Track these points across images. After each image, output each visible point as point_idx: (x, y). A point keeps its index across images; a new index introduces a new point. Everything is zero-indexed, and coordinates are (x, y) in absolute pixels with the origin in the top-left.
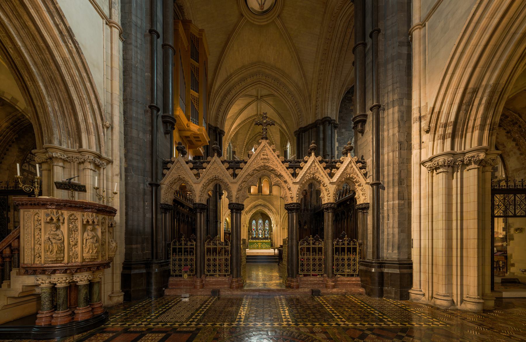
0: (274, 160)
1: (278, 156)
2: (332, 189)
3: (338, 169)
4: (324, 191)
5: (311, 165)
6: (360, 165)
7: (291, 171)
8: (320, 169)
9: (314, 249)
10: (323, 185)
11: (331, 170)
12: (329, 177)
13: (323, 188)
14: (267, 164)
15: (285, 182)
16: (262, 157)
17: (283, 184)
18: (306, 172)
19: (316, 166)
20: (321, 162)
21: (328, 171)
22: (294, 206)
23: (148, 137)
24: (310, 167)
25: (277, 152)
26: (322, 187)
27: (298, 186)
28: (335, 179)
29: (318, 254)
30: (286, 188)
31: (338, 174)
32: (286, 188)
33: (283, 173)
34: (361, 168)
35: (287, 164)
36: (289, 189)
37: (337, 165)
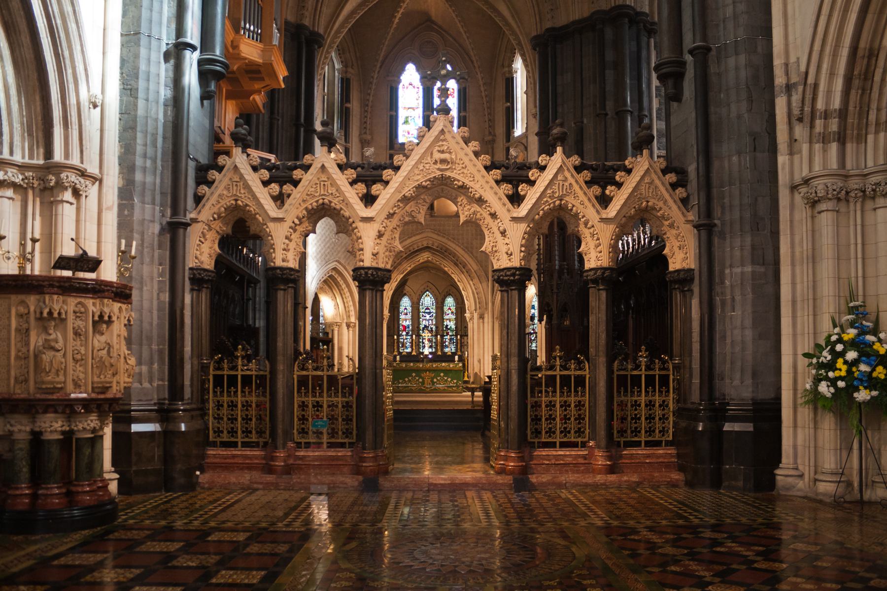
0: (467, 162)
1: (477, 154)
3: (619, 185)
4: (589, 239)
5: (556, 176)
8: (576, 187)
9: (566, 380)
10: (586, 224)
12: (597, 206)
13: (585, 233)
14: (448, 174)
16: (437, 156)
17: (489, 219)
19: (566, 179)
20: (578, 169)
21: (596, 190)
22: (514, 275)
24: (551, 181)
25: (474, 145)
26: (582, 227)
29: (576, 391)
30: (495, 229)
31: (619, 198)
32: (495, 229)
36: (503, 233)
37: (617, 178)
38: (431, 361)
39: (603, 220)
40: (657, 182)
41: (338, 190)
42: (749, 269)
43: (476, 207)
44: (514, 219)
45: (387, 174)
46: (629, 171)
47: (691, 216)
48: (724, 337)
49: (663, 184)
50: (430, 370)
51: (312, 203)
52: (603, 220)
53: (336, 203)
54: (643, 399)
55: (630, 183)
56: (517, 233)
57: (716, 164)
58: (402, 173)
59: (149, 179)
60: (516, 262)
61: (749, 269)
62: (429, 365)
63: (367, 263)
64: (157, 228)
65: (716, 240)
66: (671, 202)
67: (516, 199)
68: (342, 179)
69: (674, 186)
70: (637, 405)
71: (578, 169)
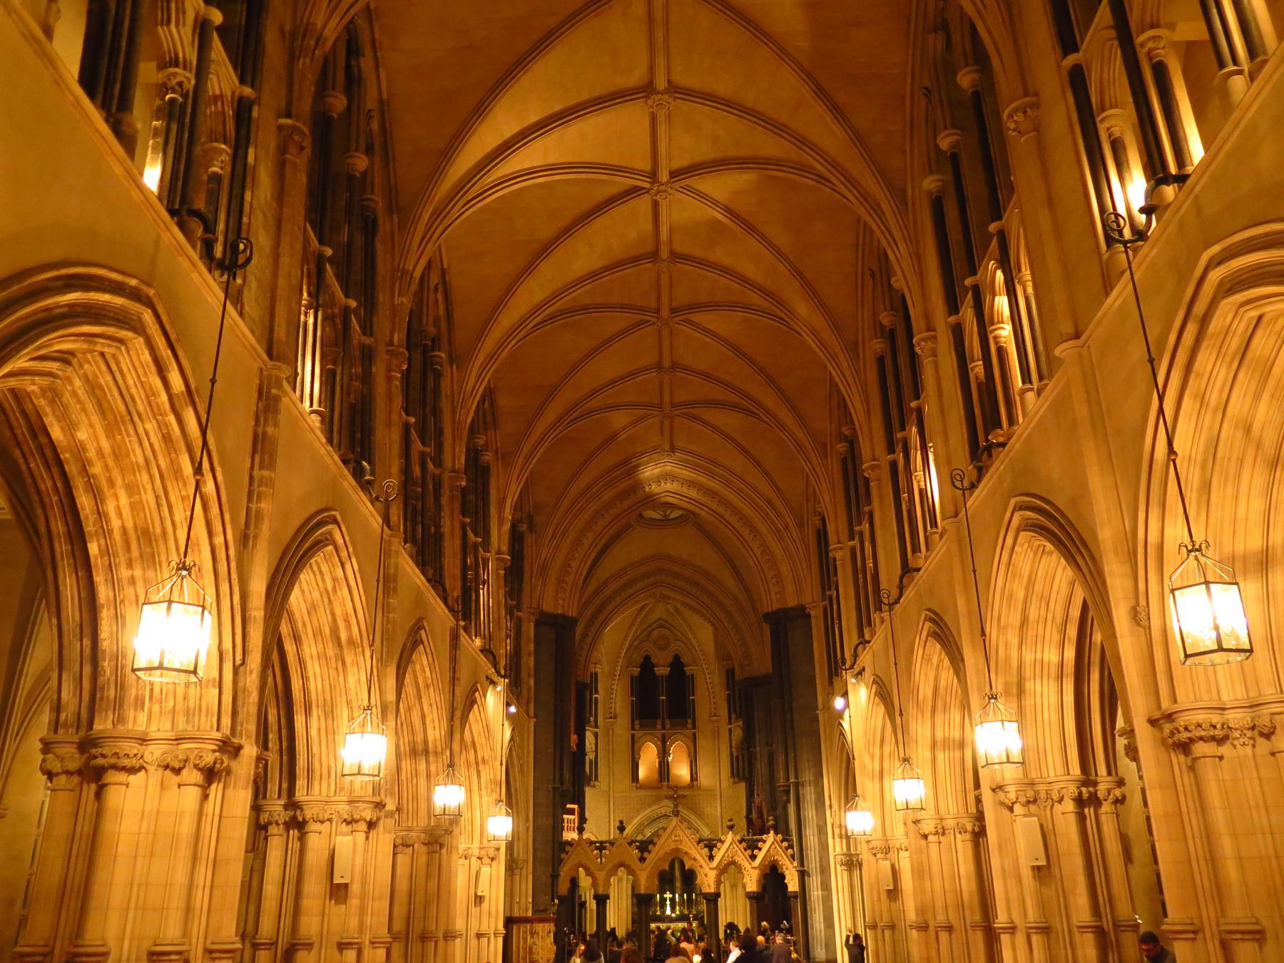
3: (760, 849)
6: (785, 844)
8: (739, 851)
11: (753, 851)
15: (701, 867)
16: (674, 838)
21: (749, 852)
23: (550, 821)
27: (715, 872)
28: (757, 862)
33: (698, 857)
34: (787, 848)
36: (706, 875)
39: (753, 868)
40: (778, 848)
43: (693, 862)
44: (711, 869)
45: (651, 847)
46: (764, 842)
47: (795, 864)
49: (781, 848)
51: (616, 862)
52: (753, 868)
53: (628, 863)
55: (765, 848)
56: (712, 875)
58: (657, 848)
60: (712, 890)
63: (643, 892)
66: (785, 857)
67: (711, 858)
69: (787, 848)
71: (740, 842)
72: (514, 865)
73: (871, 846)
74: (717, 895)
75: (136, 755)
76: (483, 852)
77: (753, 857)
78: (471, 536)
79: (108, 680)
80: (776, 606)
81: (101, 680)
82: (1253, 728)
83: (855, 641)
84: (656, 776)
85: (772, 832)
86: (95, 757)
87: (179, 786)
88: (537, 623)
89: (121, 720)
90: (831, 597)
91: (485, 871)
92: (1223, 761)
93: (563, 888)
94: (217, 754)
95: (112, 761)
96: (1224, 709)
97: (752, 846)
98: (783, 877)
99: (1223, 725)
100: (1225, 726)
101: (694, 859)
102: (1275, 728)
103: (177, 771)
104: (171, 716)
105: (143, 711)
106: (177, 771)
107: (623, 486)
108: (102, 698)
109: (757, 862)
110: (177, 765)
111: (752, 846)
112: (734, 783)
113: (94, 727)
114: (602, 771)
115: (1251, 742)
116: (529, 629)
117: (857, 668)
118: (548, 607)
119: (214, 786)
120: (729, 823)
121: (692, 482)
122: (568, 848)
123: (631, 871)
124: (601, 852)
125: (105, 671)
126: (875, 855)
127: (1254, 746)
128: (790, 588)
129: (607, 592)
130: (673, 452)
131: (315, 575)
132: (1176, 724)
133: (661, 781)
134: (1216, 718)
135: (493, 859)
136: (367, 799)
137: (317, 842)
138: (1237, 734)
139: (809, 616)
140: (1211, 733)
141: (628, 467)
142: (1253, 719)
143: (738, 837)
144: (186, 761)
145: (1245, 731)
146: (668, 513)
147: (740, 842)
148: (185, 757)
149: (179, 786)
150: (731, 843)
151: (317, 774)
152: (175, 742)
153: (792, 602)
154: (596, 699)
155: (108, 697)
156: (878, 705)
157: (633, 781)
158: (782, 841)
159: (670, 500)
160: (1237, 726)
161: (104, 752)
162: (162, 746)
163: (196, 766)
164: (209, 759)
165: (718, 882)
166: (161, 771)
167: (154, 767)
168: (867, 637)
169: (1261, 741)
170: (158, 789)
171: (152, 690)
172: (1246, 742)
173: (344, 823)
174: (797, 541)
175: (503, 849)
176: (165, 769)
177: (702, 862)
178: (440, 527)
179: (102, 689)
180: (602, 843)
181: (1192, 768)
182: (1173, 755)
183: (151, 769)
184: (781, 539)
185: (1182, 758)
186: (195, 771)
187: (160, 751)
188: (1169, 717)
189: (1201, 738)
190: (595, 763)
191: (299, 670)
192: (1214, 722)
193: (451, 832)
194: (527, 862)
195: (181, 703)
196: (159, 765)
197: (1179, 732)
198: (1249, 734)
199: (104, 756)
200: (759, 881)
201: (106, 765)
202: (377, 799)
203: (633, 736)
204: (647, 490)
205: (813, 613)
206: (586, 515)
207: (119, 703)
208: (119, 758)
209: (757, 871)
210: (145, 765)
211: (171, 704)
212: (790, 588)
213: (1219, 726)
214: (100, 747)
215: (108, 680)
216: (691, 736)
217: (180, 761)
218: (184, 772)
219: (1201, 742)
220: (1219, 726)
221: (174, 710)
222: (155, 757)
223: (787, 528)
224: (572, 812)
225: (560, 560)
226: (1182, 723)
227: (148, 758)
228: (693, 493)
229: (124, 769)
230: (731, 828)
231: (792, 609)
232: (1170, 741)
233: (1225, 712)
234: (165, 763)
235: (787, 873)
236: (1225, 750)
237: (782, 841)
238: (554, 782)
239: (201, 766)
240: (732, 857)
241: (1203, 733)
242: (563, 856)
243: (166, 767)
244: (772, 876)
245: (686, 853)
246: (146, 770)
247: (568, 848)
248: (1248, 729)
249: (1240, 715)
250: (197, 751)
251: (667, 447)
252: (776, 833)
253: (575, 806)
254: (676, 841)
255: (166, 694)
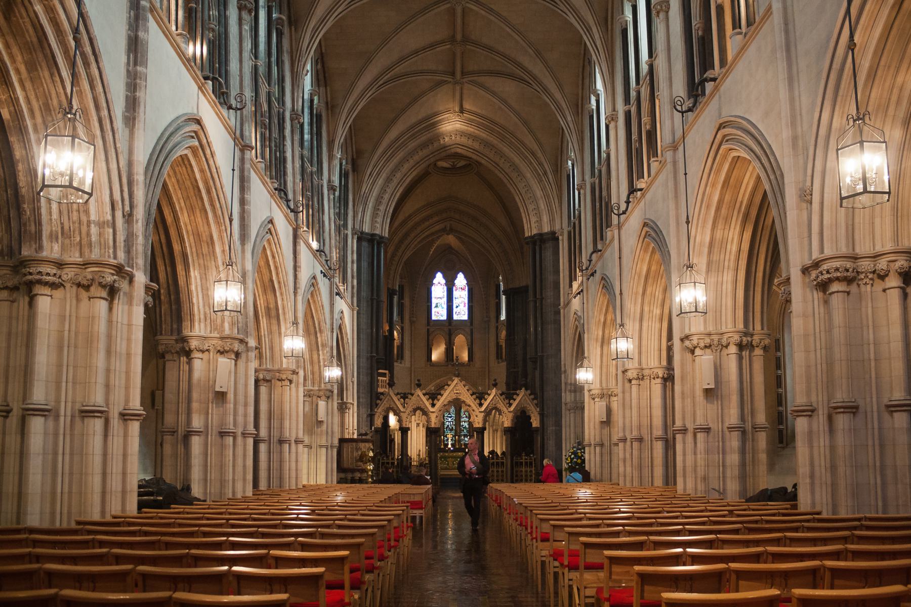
1: (468, 390)
2: (510, 416)
3: (515, 400)
6: (532, 397)
7: (478, 401)
8: (500, 401)
11: (510, 401)
15: (473, 410)
16: (455, 391)
18: (489, 404)
21: (507, 401)
23: (369, 379)
28: (512, 408)
33: (472, 405)
34: (533, 399)
35: (474, 396)
36: (477, 416)
38: (452, 451)
39: (509, 412)
41: (423, 402)
42: (554, 428)
46: (518, 395)
47: (538, 410)
48: (547, 450)
50: (452, 457)
51: (415, 407)
52: (509, 412)
53: (422, 407)
54: (524, 469)
57: (545, 393)
58: (444, 397)
59: (364, 400)
60: (480, 425)
61: (554, 428)
62: (451, 454)
64: (365, 416)
65: (545, 419)
67: (481, 405)
68: (424, 399)
69: (533, 399)
70: (521, 471)
71: (501, 395)
72: (344, 406)
73: (591, 393)
74: (484, 429)
75: (55, 275)
76: (321, 393)
77: (510, 405)
78: (307, 165)
79: (29, 218)
80: (535, 232)
81: (25, 218)
82: (874, 272)
83: (590, 248)
84: (443, 357)
85: (523, 389)
86: (25, 275)
87: (90, 298)
88: (360, 240)
89: (40, 248)
90: (574, 224)
91: (322, 404)
92: (851, 295)
93: (378, 422)
94: (115, 277)
95: (38, 277)
96: (856, 259)
97: (509, 396)
98: (530, 418)
99: (854, 270)
100: (855, 270)
101: (469, 406)
102: (889, 271)
103: (87, 288)
104: (78, 248)
105: (58, 243)
106: (87, 288)
107: (423, 138)
108: (25, 231)
109: (512, 408)
110: (85, 282)
111: (509, 396)
112: (498, 363)
113: (22, 253)
114: (407, 354)
115: (871, 282)
116: (352, 243)
117: (590, 272)
118: (367, 229)
119: (116, 301)
120: (494, 383)
121: (475, 137)
122: (382, 397)
123: (425, 413)
124: (404, 400)
125: (25, 211)
126: (594, 399)
127: (872, 285)
128: (545, 219)
129: (410, 224)
130: (463, 113)
131: (186, 168)
132: (820, 269)
133: (447, 361)
134: (849, 265)
135: (328, 398)
136: (233, 336)
137: (198, 365)
138: (862, 276)
139: (558, 239)
140: (845, 275)
141: (429, 123)
142: (875, 265)
143: (500, 392)
144: (93, 280)
145: (868, 274)
146: (456, 163)
147: (501, 395)
148: (91, 277)
149: (90, 298)
150: (495, 396)
151: (197, 318)
152: (83, 267)
153: (546, 229)
154: (402, 303)
155: (30, 232)
156: (604, 295)
157: (428, 361)
158: (530, 395)
159: (459, 151)
160: (863, 270)
161: (31, 271)
162: (73, 269)
163: (100, 284)
164: (109, 279)
165: (485, 420)
166: (75, 288)
167: (69, 285)
168: (599, 247)
169: (877, 281)
170: (74, 302)
171: (62, 228)
172: (868, 282)
173: (218, 354)
174: (553, 185)
175: (336, 391)
176: (78, 287)
177: (475, 408)
178: (284, 152)
179: (25, 224)
180: (405, 394)
181: (826, 302)
182: (815, 293)
183: (68, 285)
184: (540, 181)
185: (821, 294)
186: (100, 288)
187: (73, 273)
188: (816, 265)
189: (837, 279)
190: (401, 347)
191: (179, 242)
192: (848, 266)
193: (297, 373)
194: (353, 404)
195: (86, 239)
196: (73, 283)
197: (822, 274)
198: (871, 276)
199: (31, 274)
200: (512, 420)
201: (34, 280)
202: (241, 336)
203: (428, 330)
204: (442, 142)
205: (560, 238)
206: (395, 160)
207: (38, 236)
208: (42, 275)
209: (512, 414)
210: (63, 283)
211: (78, 239)
212: (545, 219)
213: (851, 270)
214: (29, 268)
215: (29, 218)
216: (469, 333)
217: (88, 280)
218: (92, 289)
219: (837, 282)
220: (851, 270)
221: (80, 243)
222: (69, 276)
223: (545, 173)
224: (384, 375)
225: (375, 193)
226: (825, 268)
227: (65, 277)
228: (476, 145)
229: (46, 284)
230: (495, 385)
231: (546, 233)
232: (815, 283)
233: (857, 261)
234: (77, 282)
235: (532, 415)
236: (853, 288)
237: (530, 395)
238: (371, 353)
239: (104, 283)
240: (495, 405)
241: (839, 274)
242: (378, 401)
243: (79, 285)
244: (522, 418)
245: (464, 402)
246: (64, 287)
247: (382, 397)
248: (871, 273)
249: (868, 263)
250: (99, 273)
251: (457, 109)
252: (526, 389)
253: (387, 372)
254: (457, 393)
255: (74, 232)
